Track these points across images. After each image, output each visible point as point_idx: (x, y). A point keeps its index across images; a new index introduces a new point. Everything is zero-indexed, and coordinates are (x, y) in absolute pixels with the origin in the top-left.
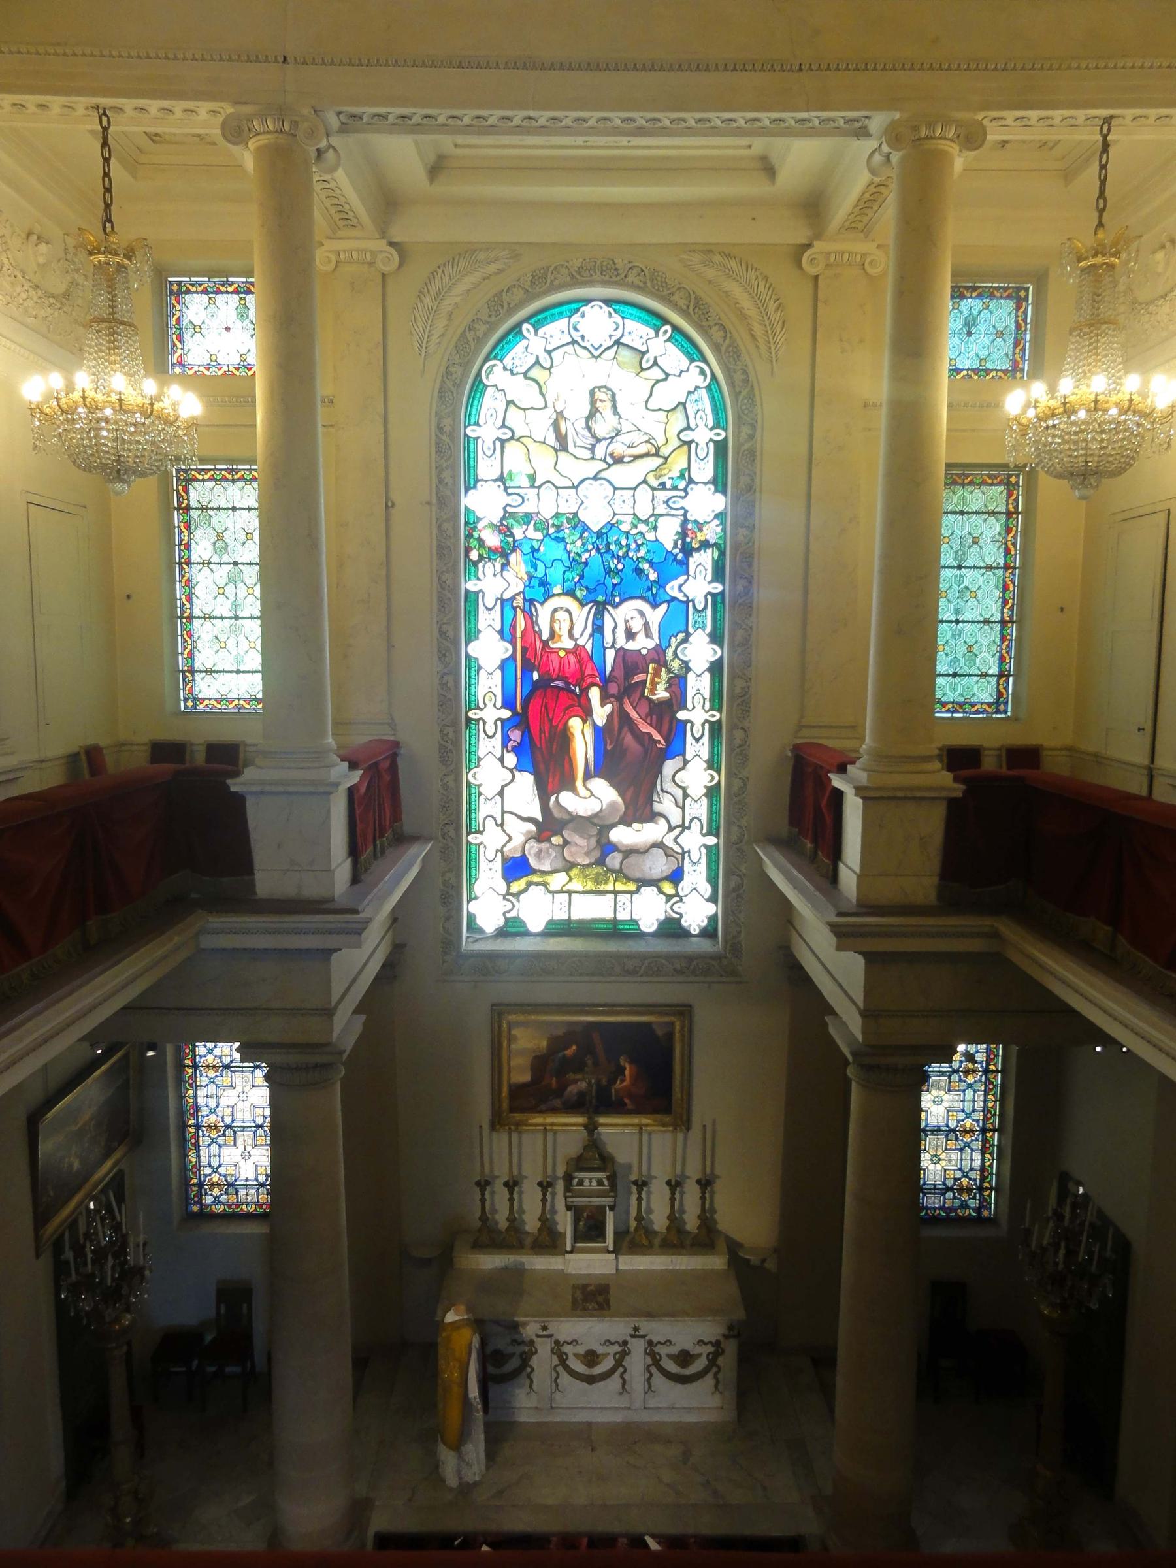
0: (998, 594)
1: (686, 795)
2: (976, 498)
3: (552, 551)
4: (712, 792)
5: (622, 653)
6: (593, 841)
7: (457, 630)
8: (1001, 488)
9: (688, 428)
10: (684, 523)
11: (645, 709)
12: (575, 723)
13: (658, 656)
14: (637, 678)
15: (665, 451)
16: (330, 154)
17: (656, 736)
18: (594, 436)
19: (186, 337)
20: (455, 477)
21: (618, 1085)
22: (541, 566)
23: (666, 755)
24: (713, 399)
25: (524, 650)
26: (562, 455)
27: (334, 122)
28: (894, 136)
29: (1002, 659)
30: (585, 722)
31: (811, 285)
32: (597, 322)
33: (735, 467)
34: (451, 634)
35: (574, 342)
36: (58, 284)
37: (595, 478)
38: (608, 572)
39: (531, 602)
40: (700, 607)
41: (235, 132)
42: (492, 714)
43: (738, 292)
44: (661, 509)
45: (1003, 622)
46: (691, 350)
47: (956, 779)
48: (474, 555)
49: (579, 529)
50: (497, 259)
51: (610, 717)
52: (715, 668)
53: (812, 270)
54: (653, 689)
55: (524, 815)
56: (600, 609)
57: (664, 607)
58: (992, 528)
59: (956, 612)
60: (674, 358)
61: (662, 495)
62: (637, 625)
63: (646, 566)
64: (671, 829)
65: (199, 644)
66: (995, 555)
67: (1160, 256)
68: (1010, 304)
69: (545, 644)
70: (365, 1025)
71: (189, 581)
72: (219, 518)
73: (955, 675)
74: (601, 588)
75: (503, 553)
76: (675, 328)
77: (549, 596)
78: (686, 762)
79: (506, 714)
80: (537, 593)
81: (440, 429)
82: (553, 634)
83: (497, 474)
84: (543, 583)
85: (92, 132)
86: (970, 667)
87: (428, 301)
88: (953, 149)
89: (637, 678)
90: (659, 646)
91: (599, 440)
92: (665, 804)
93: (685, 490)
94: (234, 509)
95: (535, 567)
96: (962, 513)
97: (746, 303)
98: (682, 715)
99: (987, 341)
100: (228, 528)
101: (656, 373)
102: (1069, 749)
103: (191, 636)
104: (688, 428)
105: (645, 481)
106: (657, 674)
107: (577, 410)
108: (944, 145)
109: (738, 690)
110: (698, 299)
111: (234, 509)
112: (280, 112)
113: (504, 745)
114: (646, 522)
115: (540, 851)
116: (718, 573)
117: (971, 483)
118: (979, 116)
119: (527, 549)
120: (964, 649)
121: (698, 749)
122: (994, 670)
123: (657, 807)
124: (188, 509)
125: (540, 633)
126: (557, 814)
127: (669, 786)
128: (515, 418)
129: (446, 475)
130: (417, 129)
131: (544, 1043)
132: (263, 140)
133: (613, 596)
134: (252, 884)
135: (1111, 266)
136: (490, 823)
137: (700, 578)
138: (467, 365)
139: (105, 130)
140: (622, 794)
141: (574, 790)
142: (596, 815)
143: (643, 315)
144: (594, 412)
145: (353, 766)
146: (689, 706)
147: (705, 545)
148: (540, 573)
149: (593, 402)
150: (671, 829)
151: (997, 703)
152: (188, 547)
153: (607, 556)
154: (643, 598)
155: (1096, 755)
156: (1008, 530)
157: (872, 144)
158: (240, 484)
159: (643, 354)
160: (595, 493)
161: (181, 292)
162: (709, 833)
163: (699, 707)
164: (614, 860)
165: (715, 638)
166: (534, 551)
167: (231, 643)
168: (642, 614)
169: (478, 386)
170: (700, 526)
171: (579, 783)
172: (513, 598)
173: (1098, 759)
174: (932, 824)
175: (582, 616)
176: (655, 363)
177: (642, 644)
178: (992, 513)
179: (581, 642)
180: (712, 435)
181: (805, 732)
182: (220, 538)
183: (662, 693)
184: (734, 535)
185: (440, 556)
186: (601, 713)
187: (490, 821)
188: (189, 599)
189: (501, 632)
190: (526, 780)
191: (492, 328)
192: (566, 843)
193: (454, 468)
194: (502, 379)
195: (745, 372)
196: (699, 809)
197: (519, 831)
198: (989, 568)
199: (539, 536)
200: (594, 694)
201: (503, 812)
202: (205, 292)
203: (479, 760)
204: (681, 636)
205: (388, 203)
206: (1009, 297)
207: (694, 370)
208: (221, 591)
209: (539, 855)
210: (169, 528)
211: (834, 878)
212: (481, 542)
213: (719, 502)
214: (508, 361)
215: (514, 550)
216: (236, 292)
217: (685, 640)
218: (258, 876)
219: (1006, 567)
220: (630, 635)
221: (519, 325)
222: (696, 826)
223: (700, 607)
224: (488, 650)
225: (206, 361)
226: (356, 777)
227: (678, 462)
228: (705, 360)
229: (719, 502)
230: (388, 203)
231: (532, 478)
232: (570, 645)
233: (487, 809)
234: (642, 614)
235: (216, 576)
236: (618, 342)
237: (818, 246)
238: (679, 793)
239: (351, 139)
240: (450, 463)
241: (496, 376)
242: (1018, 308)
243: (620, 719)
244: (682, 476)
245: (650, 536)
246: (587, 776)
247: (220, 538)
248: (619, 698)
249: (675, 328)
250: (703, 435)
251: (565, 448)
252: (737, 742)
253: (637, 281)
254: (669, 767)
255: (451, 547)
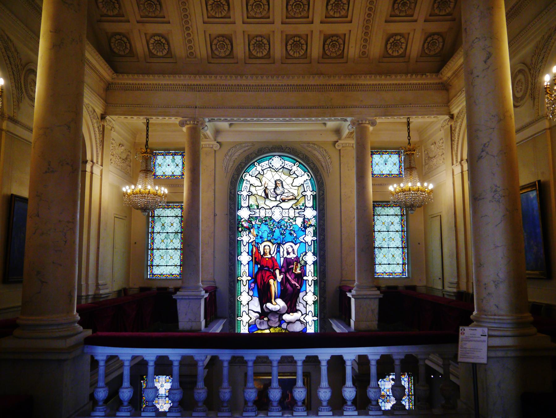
0: (400, 239)
1: (307, 304)
2: (391, 211)
3: (264, 228)
4: (314, 303)
5: (286, 259)
6: (277, 319)
7: (235, 252)
8: (399, 208)
9: (305, 191)
10: (304, 220)
11: (293, 276)
12: (271, 281)
13: (297, 260)
14: (290, 267)
15: (298, 198)
16: (206, 128)
17: (297, 285)
18: (276, 194)
19: (157, 167)
20: (235, 207)
21: (287, 401)
22: (260, 232)
23: (299, 291)
24: (311, 183)
25: (255, 258)
26: (267, 199)
27: (207, 120)
28: (353, 123)
29: (403, 259)
30: (274, 280)
31: (338, 152)
32: (277, 162)
33: (320, 202)
34: (233, 253)
35: (270, 167)
36: (124, 156)
37: (277, 206)
38: (281, 234)
39: (258, 243)
40: (310, 244)
41: (182, 124)
42: (245, 278)
43: (317, 154)
44: (297, 215)
45: (402, 248)
46: (305, 169)
47: (381, 293)
48: (240, 229)
49: (272, 221)
50: (248, 146)
51: (282, 279)
52: (314, 263)
53: (339, 148)
54: (296, 270)
55: (255, 310)
56: (279, 245)
57: (298, 244)
58: (397, 219)
59: (388, 245)
60: (299, 171)
61: (297, 211)
62: (290, 250)
63: (293, 232)
64: (302, 315)
65: (155, 257)
66: (399, 228)
67: (433, 146)
68: (397, 156)
69: (262, 256)
70: (208, 372)
71: (153, 238)
72: (163, 219)
73: (389, 264)
74: (279, 239)
75: (249, 229)
76: (300, 163)
77: (263, 242)
78: (307, 293)
79: (249, 278)
80: (259, 241)
81: (231, 193)
82: (265, 253)
83: (247, 205)
84: (261, 238)
85: (143, 123)
86: (390, 261)
87: (228, 157)
88: (369, 126)
89: (290, 267)
90: (297, 256)
91: (278, 195)
92: (300, 307)
93: (304, 209)
94: (168, 216)
95: (259, 233)
96: (388, 215)
97: (320, 157)
98: (305, 278)
99: (391, 166)
100: (169, 222)
101: (294, 176)
102: (426, 286)
103: (153, 255)
104: (305, 191)
105: (292, 207)
106: (297, 265)
107: (271, 186)
108: (366, 125)
109: (322, 270)
110: (306, 156)
111: (168, 216)
112: (194, 119)
113: (249, 289)
114: (292, 219)
115: (260, 323)
116: (315, 234)
117: (390, 206)
118: (375, 118)
119: (256, 227)
120: (391, 256)
121: (310, 289)
122: (401, 263)
123: (298, 308)
124: (154, 216)
125: (260, 253)
126: (266, 310)
127: (301, 301)
128: (253, 189)
129: (232, 206)
130: (229, 121)
131: (262, 387)
132: (189, 126)
133: (283, 241)
134: (178, 325)
135: (413, 154)
136: (244, 313)
137: (309, 236)
138: (239, 175)
139: (148, 123)
140: (286, 304)
141: (272, 303)
142: (278, 311)
143: (290, 159)
144: (276, 187)
145: (206, 292)
146: (307, 275)
147: (311, 225)
148: (260, 234)
149: (276, 184)
150: (302, 315)
151: (403, 272)
152: (153, 228)
153: (281, 229)
154: (292, 242)
155: (431, 288)
156: (402, 220)
157: (349, 123)
158: (170, 209)
159: (291, 170)
160: (277, 211)
161: (156, 155)
162: (315, 316)
163: (310, 275)
164: (284, 326)
165: (314, 254)
166: (258, 228)
167: (165, 257)
168: (292, 247)
169: (242, 180)
170: (309, 220)
171: (273, 300)
172: (252, 242)
173: (432, 289)
174: (375, 305)
175: (273, 248)
176: (294, 173)
177: (292, 256)
178: (397, 215)
179: (273, 255)
180: (311, 193)
181: (343, 282)
182: (163, 225)
183: (298, 271)
184: (319, 222)
185: (230, 230)
186: (279, 278)
187: (244, 313)
188: (153, 243)
189: (248, 253)
190: (256, 300)
191: (246, 164)
192: (269, 320)
193: (235, 204)
194: (249, 178)
195: (321, 176)
196: (311, 308)
197: (254, 316)
198: (397, 231)
199: (260, 223)
200: (277, 272)
201: (249, 310)
202: (163, 155)
203: (241, 293)
204: (304, 253)
205: (217, 132)
206: (397, 154)
207: (306, 175)
208: (163, 241)
209: (260, 324)
210: (148, 222)
211: (349, 324)
212: (242, 225)
213: (315, 213)
214: (250, 173)
215: (252, 228)
216: (172, 155)
217: (305, 255)
218: (180, 323)
219: (402, 231)
220: (288, 253)
221: (254, 163)
222: (310, 314)
223: (310, 244)
224: (245, 258)
225: (162, 174)
226: (207, 295)
227: (302, 202)
228: (309, 172)
229: (315, 213)
230: (217, 132)
231: (258, 206)
232: (270, 256)
233: (244, 309)
234: (292, 247)
235: (162, 236)
236: (283, 167)
237: (340, 142)
238: (305, 303)
239: (211, 123)
240: (233, 203)
241: (248, 177)
242: (399, 157)
243: (285, 281)
244: (303, 205)
245: (294, 223)
246: (275, 298)
247: (163, 225)
248: (285, 273)
249: (300, 163)
250: (309, 193)
251: (268, 198)
252: (322, 286)
253: (288, 151)
254: (301, 295)
255: (234, 226)
